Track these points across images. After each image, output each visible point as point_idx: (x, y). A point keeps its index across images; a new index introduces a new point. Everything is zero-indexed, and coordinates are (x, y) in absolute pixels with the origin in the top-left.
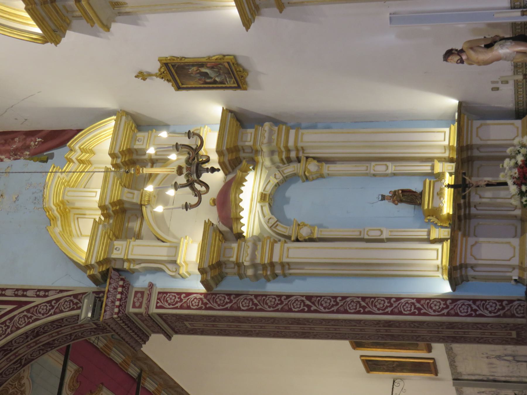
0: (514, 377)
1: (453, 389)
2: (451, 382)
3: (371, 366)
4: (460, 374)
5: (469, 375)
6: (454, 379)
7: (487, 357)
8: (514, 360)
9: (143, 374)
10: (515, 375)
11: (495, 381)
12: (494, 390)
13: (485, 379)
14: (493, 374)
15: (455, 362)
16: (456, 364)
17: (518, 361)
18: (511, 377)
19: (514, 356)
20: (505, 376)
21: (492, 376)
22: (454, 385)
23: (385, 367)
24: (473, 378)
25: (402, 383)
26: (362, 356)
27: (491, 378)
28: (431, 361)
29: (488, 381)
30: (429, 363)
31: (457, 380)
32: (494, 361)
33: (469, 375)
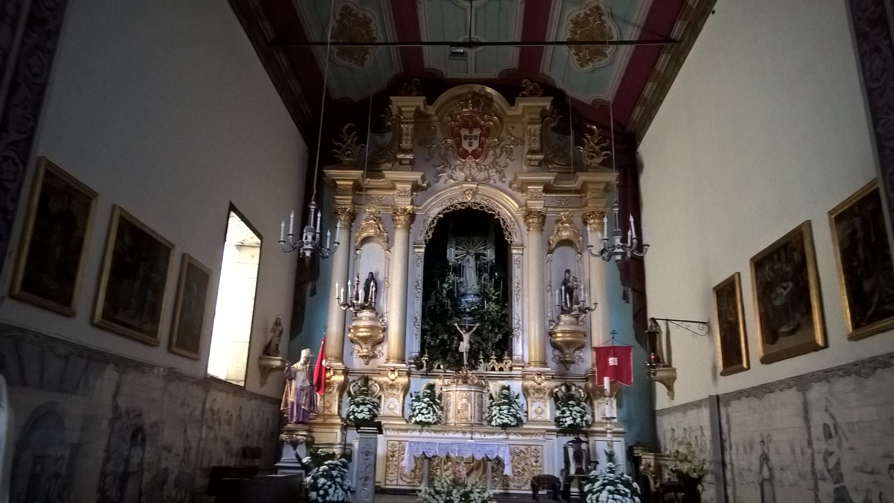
0: (733, 475)
1: (703, 395)
2: (714, 393)
3: (726, 293)
4: (728, 404)
5: (728, 416)
6: (718, 397)
7: (763, 442)
8: (764, 480)
9: (676, 45)
10: (737, 479)
11: (723, 449)
12: (709, 446)
13: (724, 437)
14: (734, 447)
15: (747, 397)
16: (744, 401)
17: (762, 485)
18: (732, 470)
19: (771, 479)
20: (732, 464)
21: (731, 447)
22: (710, 396)
23: (725, 308)
24: (724, 421)
25: (704, 332)
26: (739, 274)
27: (727, 445)
28: (745, 365)
29: (722, 441)
30: (741, 362)
31: (717, 402)
32: (758, 450)
33: (728, 416)
